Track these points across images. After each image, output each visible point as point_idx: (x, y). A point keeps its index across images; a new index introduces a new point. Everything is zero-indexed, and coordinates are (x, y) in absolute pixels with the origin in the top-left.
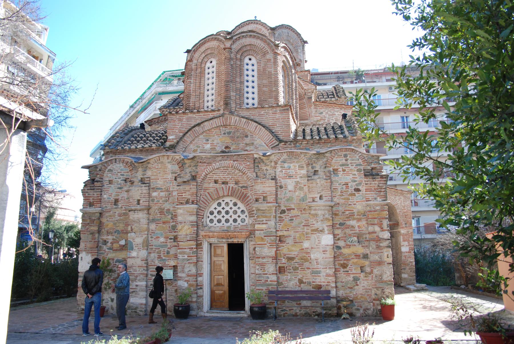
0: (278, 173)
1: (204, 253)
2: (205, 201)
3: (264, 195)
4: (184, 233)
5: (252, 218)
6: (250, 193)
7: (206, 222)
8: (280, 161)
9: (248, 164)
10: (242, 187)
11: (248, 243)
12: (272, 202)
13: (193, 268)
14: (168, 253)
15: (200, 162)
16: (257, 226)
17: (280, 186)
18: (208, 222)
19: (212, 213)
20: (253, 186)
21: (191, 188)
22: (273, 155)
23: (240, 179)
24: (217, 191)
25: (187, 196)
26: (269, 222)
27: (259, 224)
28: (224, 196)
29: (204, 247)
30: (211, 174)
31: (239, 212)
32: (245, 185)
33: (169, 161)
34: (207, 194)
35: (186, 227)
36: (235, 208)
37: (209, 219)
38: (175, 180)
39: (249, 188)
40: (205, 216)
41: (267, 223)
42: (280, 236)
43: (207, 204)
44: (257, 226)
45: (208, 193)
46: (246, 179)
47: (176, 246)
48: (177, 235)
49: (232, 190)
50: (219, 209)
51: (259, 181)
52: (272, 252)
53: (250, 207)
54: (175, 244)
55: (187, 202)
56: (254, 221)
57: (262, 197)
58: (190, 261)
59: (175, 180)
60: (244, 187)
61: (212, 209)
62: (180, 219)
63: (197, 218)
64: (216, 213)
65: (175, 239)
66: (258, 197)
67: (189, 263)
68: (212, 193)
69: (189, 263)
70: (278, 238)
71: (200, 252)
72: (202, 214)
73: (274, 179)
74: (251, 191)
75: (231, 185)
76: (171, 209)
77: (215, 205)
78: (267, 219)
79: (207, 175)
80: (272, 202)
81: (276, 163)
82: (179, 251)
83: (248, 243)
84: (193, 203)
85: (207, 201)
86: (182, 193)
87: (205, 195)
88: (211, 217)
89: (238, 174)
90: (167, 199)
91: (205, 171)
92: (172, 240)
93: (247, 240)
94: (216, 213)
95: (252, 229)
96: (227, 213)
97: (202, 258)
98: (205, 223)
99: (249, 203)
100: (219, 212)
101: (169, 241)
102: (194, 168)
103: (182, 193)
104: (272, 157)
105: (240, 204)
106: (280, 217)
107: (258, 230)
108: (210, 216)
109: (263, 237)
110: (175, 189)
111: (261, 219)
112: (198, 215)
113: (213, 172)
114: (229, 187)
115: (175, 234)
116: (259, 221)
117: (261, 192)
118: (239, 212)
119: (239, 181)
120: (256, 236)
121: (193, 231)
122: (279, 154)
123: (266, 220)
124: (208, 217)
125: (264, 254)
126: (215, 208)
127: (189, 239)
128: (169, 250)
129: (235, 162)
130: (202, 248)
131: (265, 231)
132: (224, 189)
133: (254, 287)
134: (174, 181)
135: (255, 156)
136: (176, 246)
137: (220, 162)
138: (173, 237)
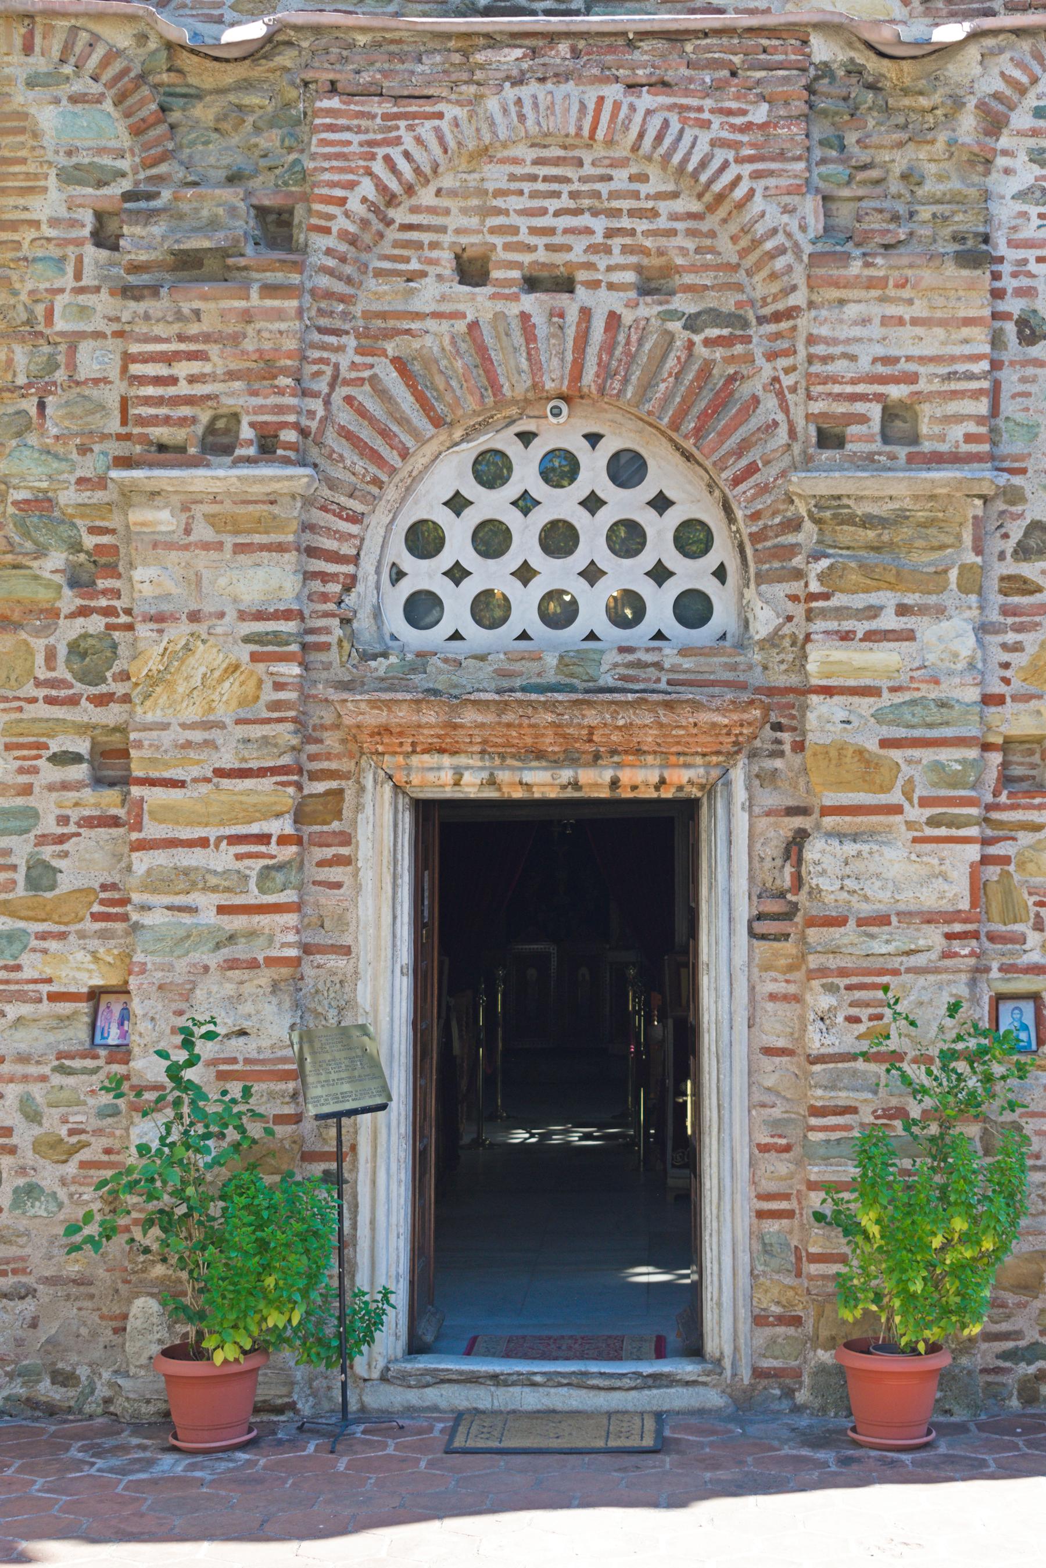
0: (1005, 211)
1: (367, 877)
2: (366, 434)
3: (896, 392)
4: (192, 713)
5: (780, 590)
6: (767, 371)
7: (377, 614)
8: (1031, 101)
9: (760, 114)
10: (692, 323)
11: (740, 794)
12: (955, 459)
13: (269, 1009)
14: (41, 876)
15: (333, 88)
16: (823, 659)
17: (1022, 323)
18: (396, 621)
19: (424, 540)
20: (790, 313)
21: (247, 317)
22: (973, 52)
23: (680, 248)
24: (482, 350)
25: (214, 382)
26: (928, 630)
27: (846, 636)
28: (537, 396)
29: (364, 834)
30: (426, 196)
31: (660, 531)
32: (728, 303)
33: (39, 63)
34: (391, 378)
35: (208, 658)
36: (625, 503)
37: (407, 587)
38: (104, 237)
39: (758, 333)
40: (367, 564)
41: (909, 636)
42: (1007, 745)
43: (392, 457)
44: (823, 659)
45: (400, 364)
46: (729, 252)
47: (114, 822)
48: (121, 729)
49: (609, 346)
50: (492, 504)
51: (856, 268)
52: (946, 878)
53: (764, 489)
54: (109, 800)
55: (218, 442)
56: (798, 610)
57: (875, 411)
58: (240, 951)
59: (104, 237)
60: (716, 317)
61: (428, 505)
62: (148, 580)
63: (309, 576)
64: (459, 546)
65: (110, 764)
66: (841, 408)
67: (232, 964)
68: (429, 361)
69: (232, 964)
70: (996, 758)
71: (334, 874)
72: (347, 549)
73: (976, 253)
74: (771, 356)
75: (603, 302)
76: (68, 497)
77: (453, 472)
78: (910, 599)
79: (391, 200)
80: (955, 459)
81: (994, 123)
82: (142, 862)
83: (740, 794)
84: (268, 445)
85: (385, 434)
86: (169, 359)
87: (373, 380)
88: (425, 574)
89: (664, 207)
90: (30, 406)
91: (378, 167)
92: (79, 772)
93: (738, 775)
94: (459, 546)
95: (780, 679)
96: (559, 539)
97: (341, 922)
98: (363, 623)
99: (753, 455)
100: (491, 539)
101: (51, 774)
102: (270, 140)
103: (169, 359)
104: (966, 67)
105: (664, 472)
106: (1016, 585)
107: (828, 691)
108: (407, 562)
109: (872, 746)
110: (98, 324)
111: (859, 601)
112: (312, 552)
113: (448, 181)
114: (586, 313)
115: (112, 715)
116: (840, 613)
117: (864, 364)
118: (660, 531)
119: (669, 270)
120: (814, 738)
121: (269, 695)
122: (1025, 45)
123: (903, 610)
124: (398, 575)
125: (880, 898)
126: (457, 503)
127: (227, 760)
128: (47, 852)
129: (646, 100)
130: (346, 839)
131: (887, 699)
132: (542, 330)
133: (781, 1166)
134: (91, 252)
135: (823, 50)
136: (114, 822)
137: (510, 93)
138: (83, 747)
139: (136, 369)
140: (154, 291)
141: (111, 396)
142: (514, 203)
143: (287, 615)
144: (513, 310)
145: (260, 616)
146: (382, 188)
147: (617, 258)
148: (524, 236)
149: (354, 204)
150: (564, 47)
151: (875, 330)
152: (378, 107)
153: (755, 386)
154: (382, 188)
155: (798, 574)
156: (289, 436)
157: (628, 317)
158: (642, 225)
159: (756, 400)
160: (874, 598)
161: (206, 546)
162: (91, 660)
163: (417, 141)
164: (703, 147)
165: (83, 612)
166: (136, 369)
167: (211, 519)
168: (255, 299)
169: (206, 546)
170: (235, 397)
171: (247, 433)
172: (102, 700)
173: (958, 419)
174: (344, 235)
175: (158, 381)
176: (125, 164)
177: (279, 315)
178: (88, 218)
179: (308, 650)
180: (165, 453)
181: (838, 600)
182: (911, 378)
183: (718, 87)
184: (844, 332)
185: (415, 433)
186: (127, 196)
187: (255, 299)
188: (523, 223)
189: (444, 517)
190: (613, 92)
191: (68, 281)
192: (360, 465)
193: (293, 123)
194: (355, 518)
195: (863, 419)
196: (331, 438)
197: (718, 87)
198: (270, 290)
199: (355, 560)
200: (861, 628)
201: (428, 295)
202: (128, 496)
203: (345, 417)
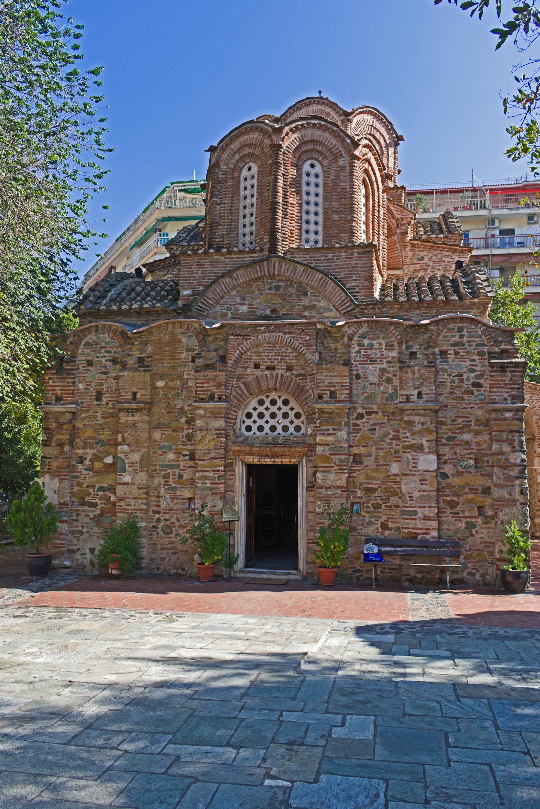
2: (237, 396)
3: (332, 389)
7: (240, 429)
9: (308, 338)
12: (342, 401)
21: (216, 376)
24: (258, 381)
28: (268, 390)
30: (249, 353)
32: (303, 372)
37: (246, 424)
43: (242, 401)
45: (244, 384)
49: (281, 380)
55: (211, 398)
57: (328, 392)
59: (193, 361)
72: (234, 418)
75: (281, 372)
76: (186, 408)
77: (254, 403)
78: (335, 427)
80: (342, 401)
84: (220, 399)
85: (241, 396)
86: (203, 383)
88: (249, 422)
89: (291, 355)
99: (308, 400)
103: (203, 383)
111: (326, 428)
113: (252, 351)
119: (292, 366)
121: (220, 444)
124: (244, 422)
129: (287, 336)
134: (191, 364)
137: (263, 335)
139: (198, 385)
140: (200, 371)
141: (194, 390)
142: (264, 354)
143: (223, 430)
144: (264, 373)
145: (218, 430)
146: (240, 352)
147: (283, 364)
148: (266, 360)
149: (236, 355)
150: (273, 327)
151: (328, 378)
152: (240, 338)
153: (308, 387)
154: (240, 352)
155: (315, 423)
156: (224, 397)
157: (285, 375)
158: (287, 358)
159: (308, 390)
160: (329, 427)
161: (209, 417)
162: (190, 437)
163: (247, 344)
164: (297, 344)
165: (188, 429)
166: (198, 385)
167: (210, 412)
168: (218, 372)
169: (209, 417)
170: (214, 390)
171: (216, 396)
172: (191, 445)
173: (344, 394)
174: (234, 360)
175: (201, 387)
176: (197, 348)
177: (222, 375)
178: (190, 357)
179: (227, 436)
180: (203, 400)
181: (322, 427)
182: (335, 386)
183: (300, 333)
184: (323, 378)
185: (246, 396)
186: (197, 354)
187: (218, 372)
188: (266, 358)
189: (252, 411)
190: (281, 334)
191: (187, 369)
192: (236, 402)
193: (226, 341)
194: (236, 412)
195: (326, 394)
196: (232, 397)
197: (300, 333)
198: (220, 371)
199: (236, 419)
200: (326, 433)
201: (249, 371)
202: (196, 408)
203: (234, 393)
